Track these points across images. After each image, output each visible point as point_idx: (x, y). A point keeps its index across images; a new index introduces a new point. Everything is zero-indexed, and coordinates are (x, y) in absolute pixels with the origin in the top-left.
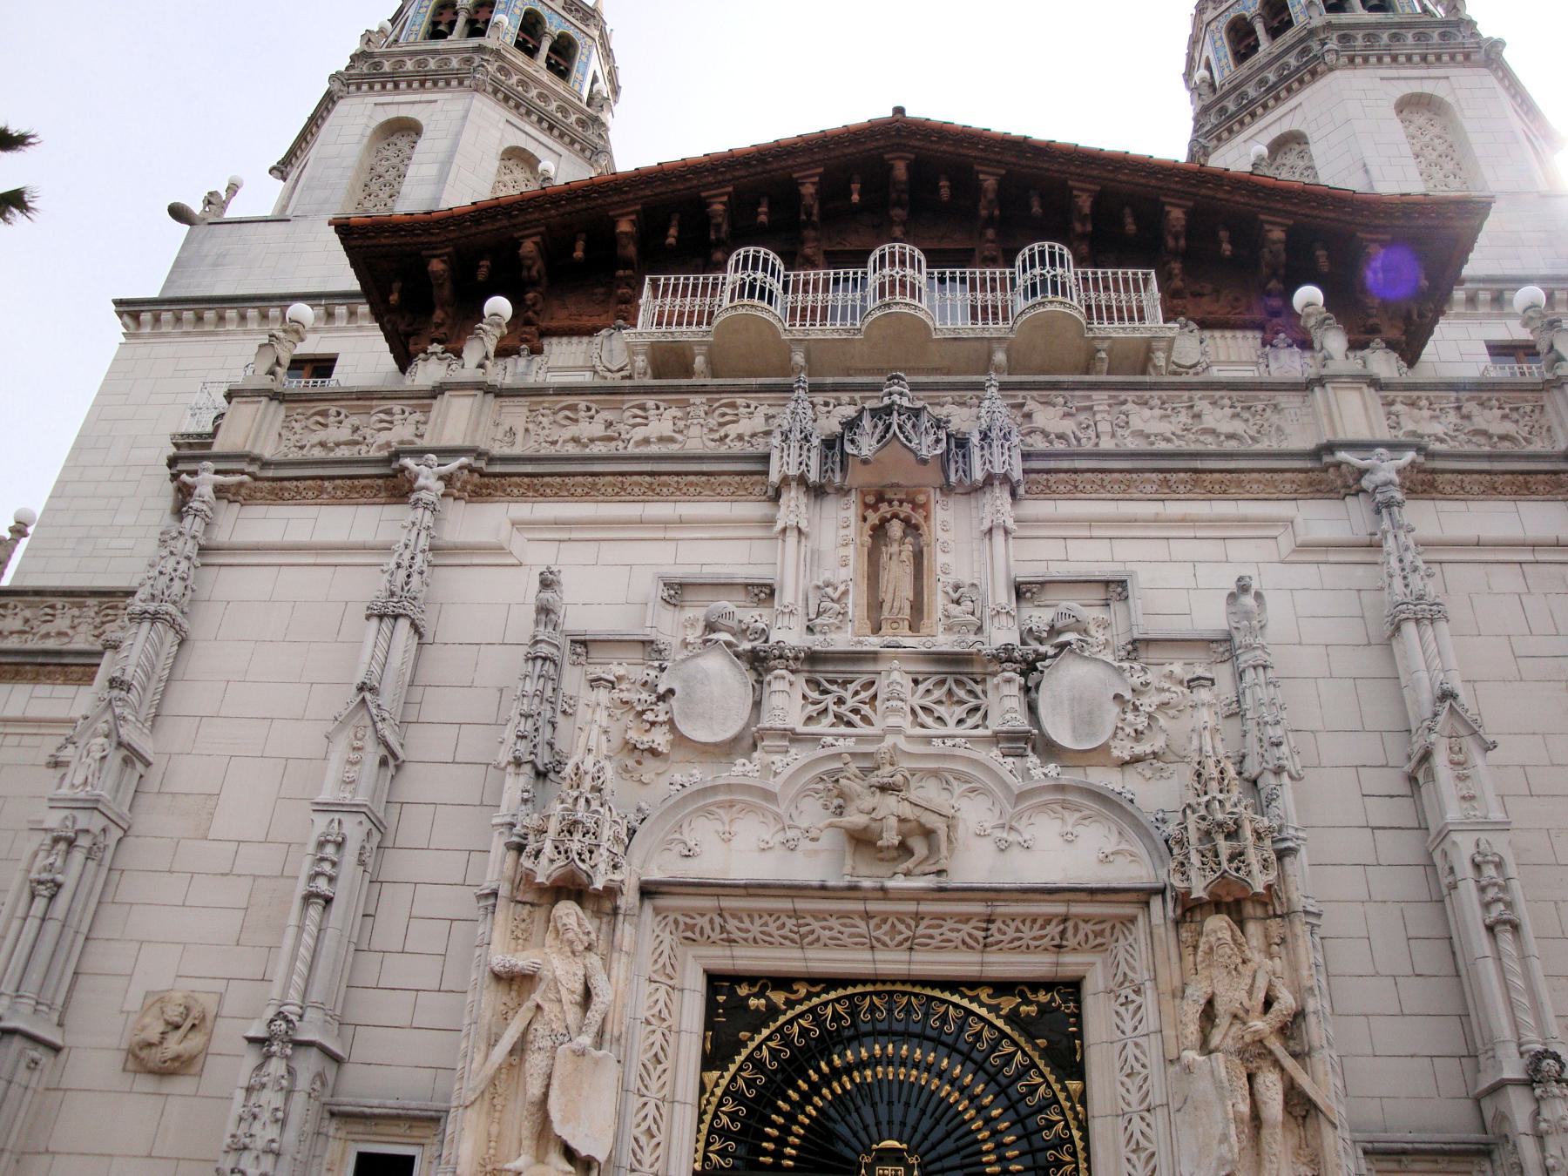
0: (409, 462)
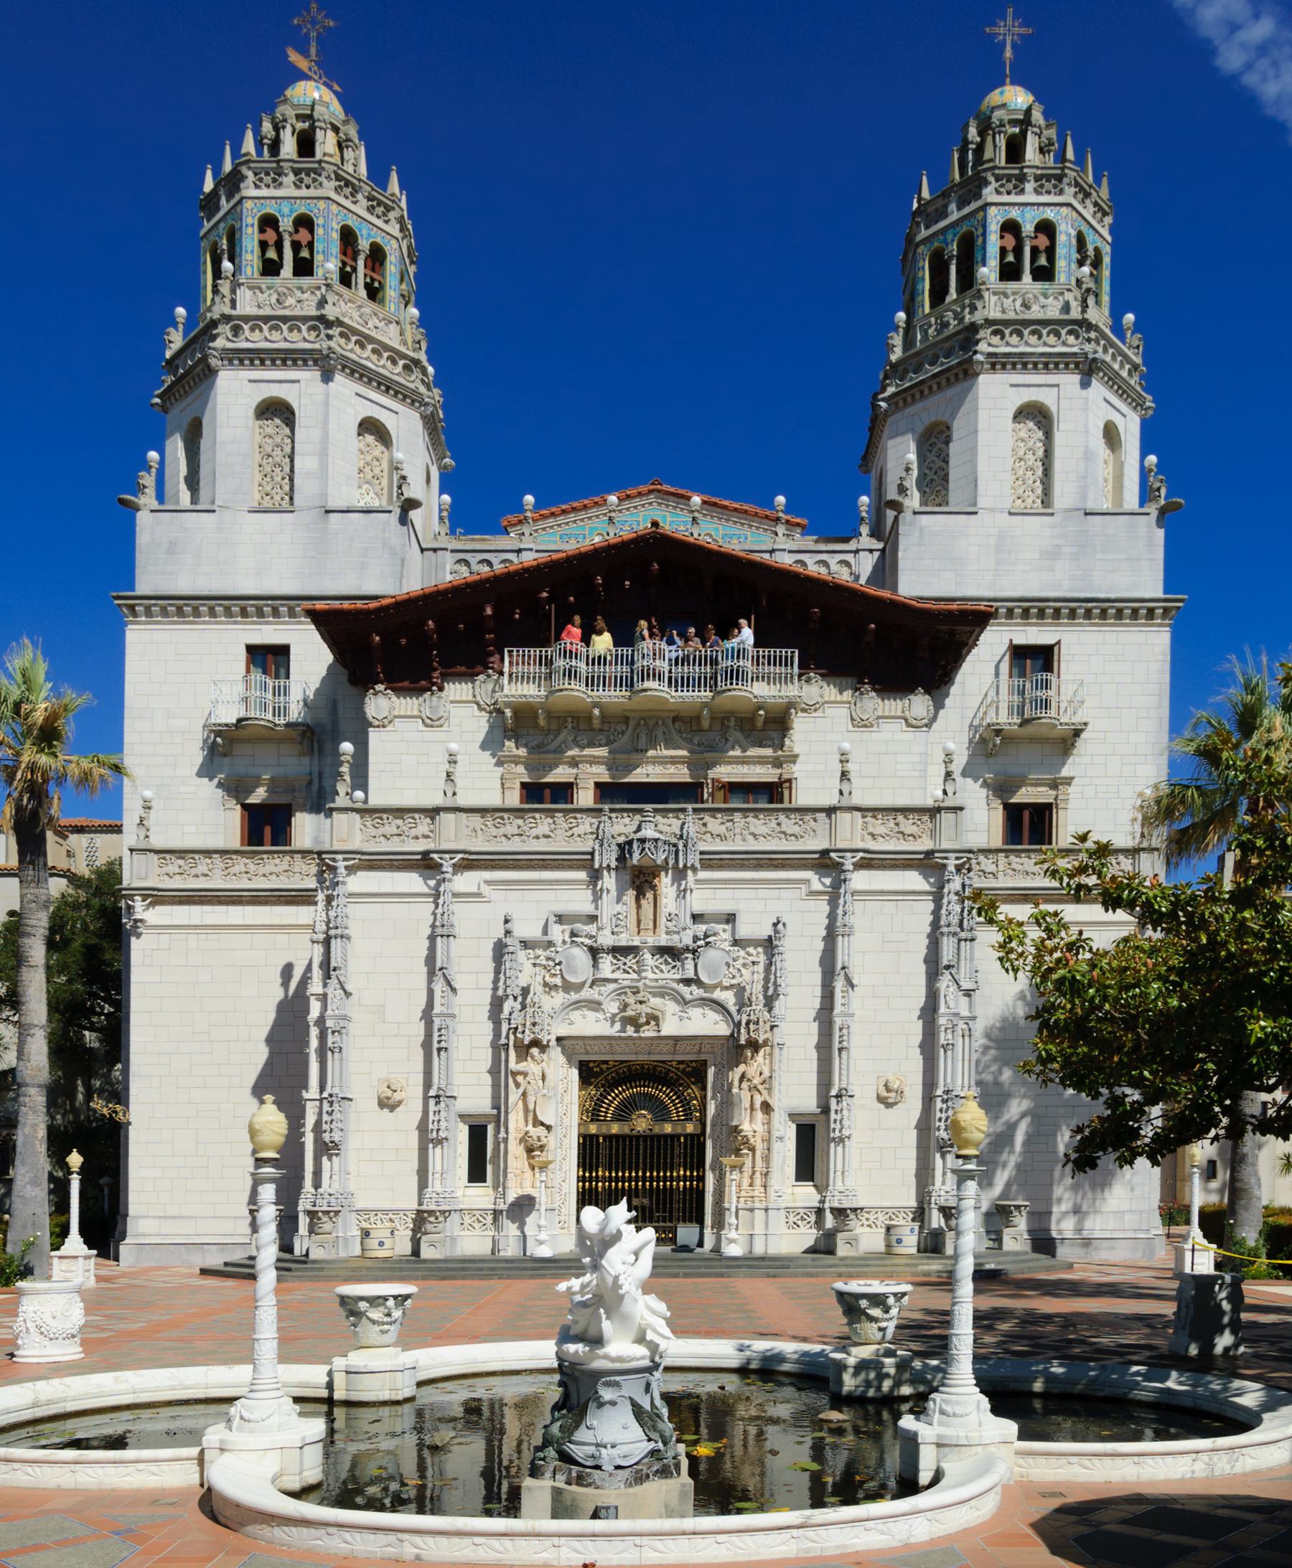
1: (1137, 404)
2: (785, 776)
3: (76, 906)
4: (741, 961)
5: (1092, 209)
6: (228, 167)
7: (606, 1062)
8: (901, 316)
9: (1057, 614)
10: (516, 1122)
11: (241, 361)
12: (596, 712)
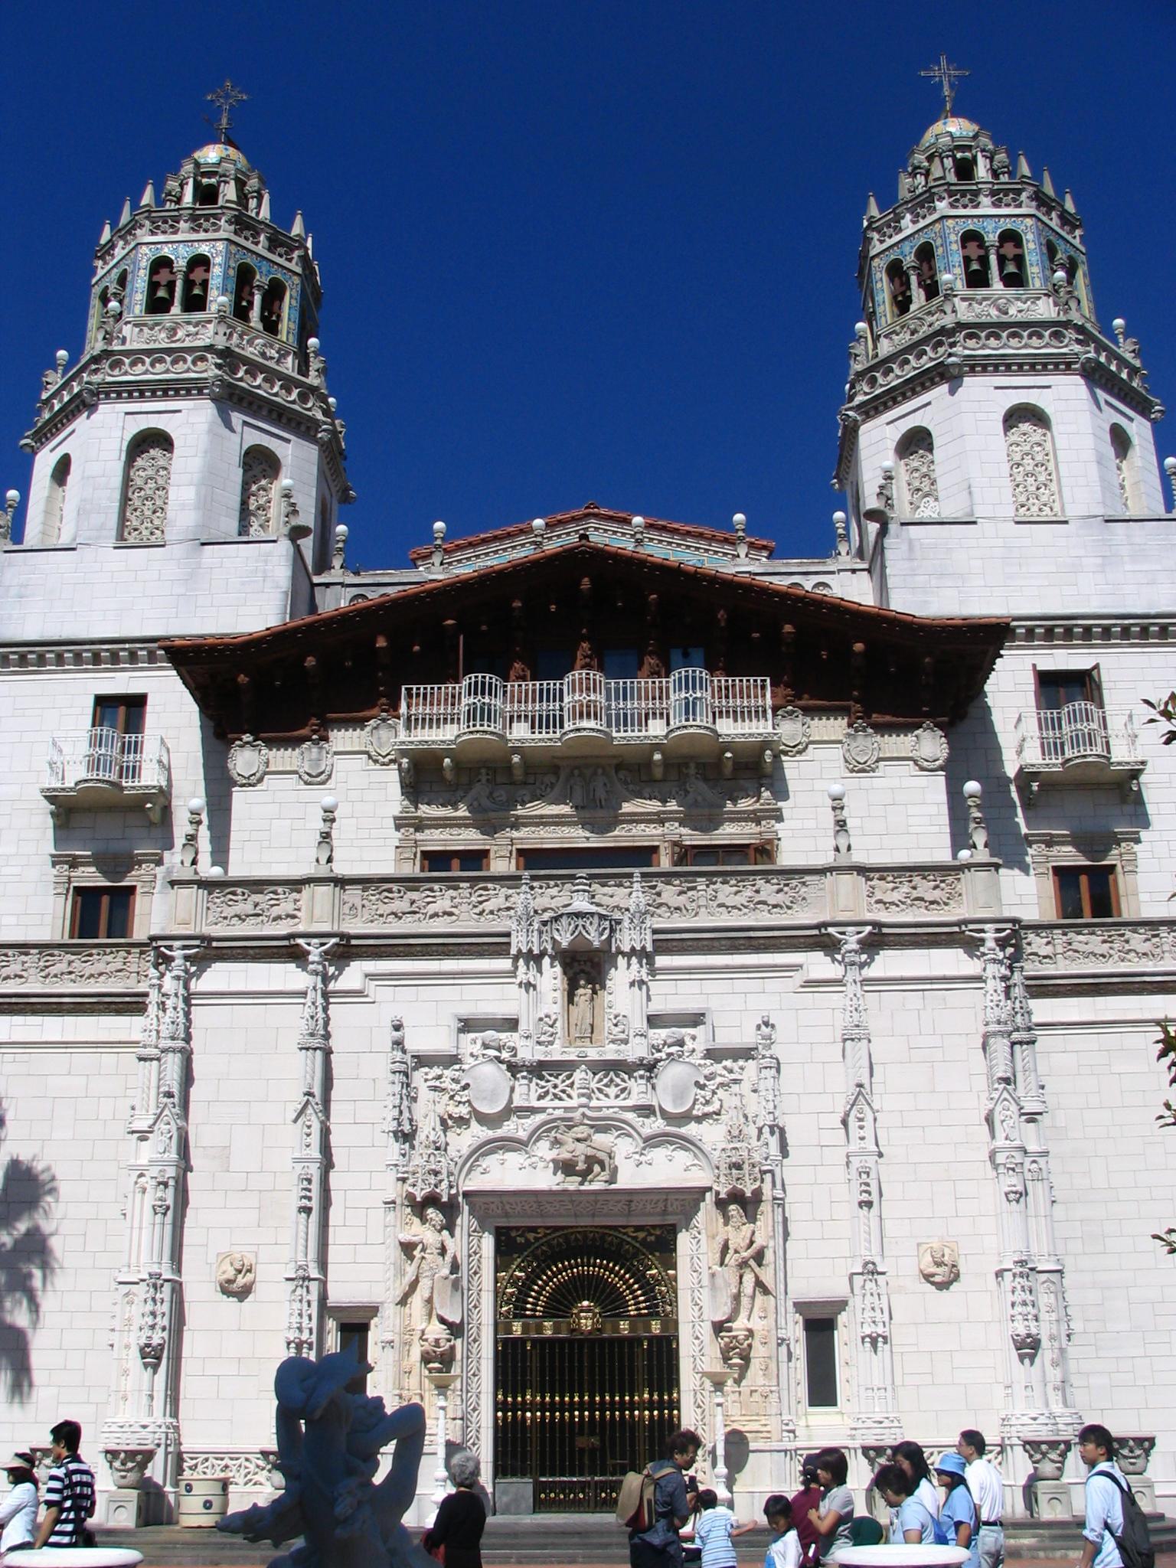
0: (301, 941)
11: (119, 395)
12: (516, 759)
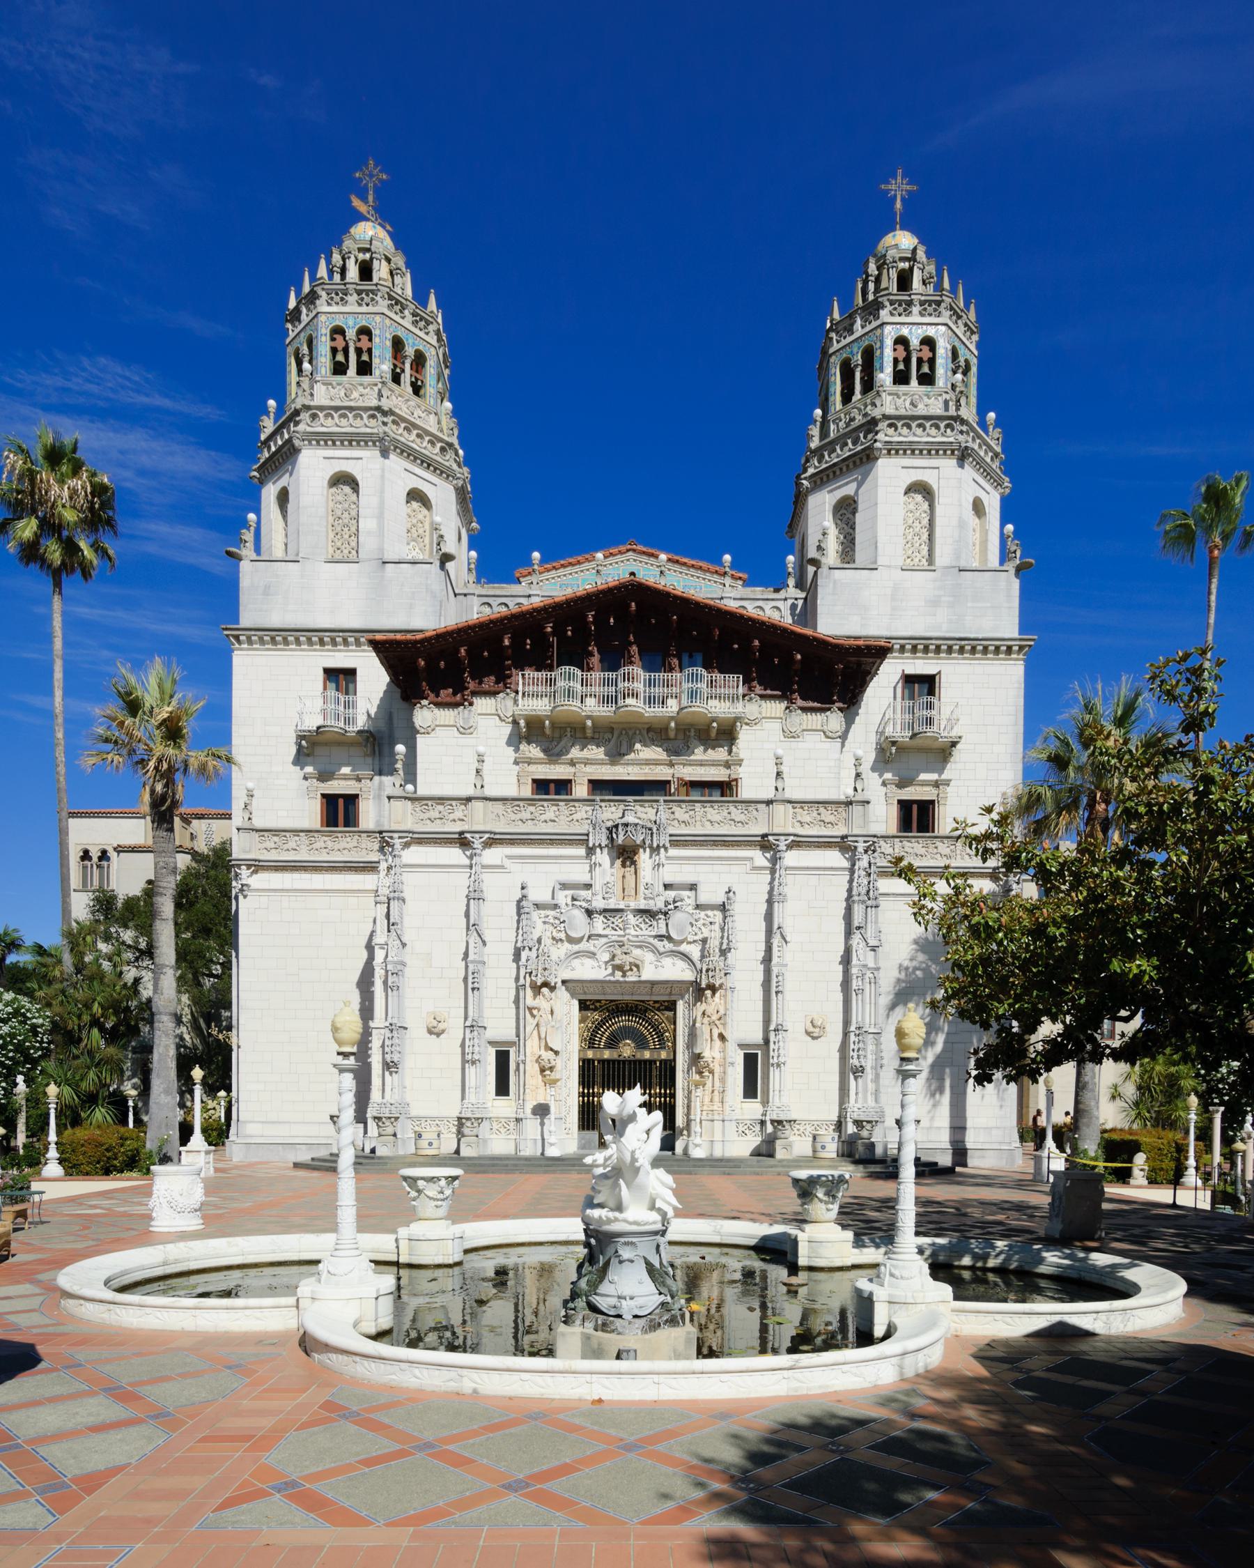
1: (998, 484)
2: (733, 777)
3: (197, 875)
4: (702, 921)
5: (963, 328)
6: (306, 288)
7: (599, 1001)
8: (818, 412)
9: (938, 649)
10: (533, 1047)
12: (589, 723)
